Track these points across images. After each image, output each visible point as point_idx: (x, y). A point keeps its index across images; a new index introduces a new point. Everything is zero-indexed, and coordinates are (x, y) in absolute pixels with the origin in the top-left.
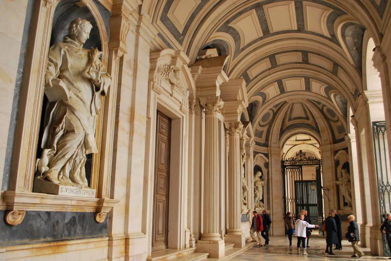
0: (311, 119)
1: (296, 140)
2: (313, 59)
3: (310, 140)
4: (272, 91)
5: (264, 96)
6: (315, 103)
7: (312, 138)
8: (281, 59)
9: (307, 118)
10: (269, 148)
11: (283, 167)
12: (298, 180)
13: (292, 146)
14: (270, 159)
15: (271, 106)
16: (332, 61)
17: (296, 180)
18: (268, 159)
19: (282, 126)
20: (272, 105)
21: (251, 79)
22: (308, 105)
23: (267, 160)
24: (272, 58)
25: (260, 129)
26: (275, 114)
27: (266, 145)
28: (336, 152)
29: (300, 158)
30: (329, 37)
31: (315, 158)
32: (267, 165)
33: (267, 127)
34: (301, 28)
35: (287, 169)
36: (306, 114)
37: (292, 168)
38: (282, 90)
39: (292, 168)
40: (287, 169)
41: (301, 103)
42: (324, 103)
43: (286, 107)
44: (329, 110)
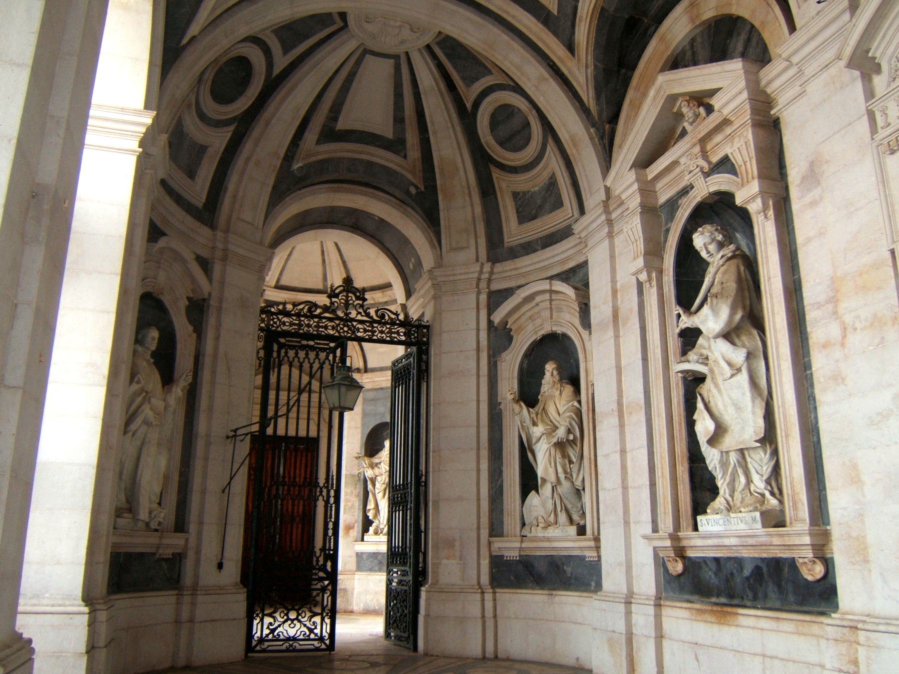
0: (414, 152)
9: (396, 145)
10: (219, 234)
11: (270, 337)
18: (210, 279)
19: (290, 156)
28: (496, 298)
32: (198, 309)
36: (399, 120)
40: (281, 346)
43: (331, 59)
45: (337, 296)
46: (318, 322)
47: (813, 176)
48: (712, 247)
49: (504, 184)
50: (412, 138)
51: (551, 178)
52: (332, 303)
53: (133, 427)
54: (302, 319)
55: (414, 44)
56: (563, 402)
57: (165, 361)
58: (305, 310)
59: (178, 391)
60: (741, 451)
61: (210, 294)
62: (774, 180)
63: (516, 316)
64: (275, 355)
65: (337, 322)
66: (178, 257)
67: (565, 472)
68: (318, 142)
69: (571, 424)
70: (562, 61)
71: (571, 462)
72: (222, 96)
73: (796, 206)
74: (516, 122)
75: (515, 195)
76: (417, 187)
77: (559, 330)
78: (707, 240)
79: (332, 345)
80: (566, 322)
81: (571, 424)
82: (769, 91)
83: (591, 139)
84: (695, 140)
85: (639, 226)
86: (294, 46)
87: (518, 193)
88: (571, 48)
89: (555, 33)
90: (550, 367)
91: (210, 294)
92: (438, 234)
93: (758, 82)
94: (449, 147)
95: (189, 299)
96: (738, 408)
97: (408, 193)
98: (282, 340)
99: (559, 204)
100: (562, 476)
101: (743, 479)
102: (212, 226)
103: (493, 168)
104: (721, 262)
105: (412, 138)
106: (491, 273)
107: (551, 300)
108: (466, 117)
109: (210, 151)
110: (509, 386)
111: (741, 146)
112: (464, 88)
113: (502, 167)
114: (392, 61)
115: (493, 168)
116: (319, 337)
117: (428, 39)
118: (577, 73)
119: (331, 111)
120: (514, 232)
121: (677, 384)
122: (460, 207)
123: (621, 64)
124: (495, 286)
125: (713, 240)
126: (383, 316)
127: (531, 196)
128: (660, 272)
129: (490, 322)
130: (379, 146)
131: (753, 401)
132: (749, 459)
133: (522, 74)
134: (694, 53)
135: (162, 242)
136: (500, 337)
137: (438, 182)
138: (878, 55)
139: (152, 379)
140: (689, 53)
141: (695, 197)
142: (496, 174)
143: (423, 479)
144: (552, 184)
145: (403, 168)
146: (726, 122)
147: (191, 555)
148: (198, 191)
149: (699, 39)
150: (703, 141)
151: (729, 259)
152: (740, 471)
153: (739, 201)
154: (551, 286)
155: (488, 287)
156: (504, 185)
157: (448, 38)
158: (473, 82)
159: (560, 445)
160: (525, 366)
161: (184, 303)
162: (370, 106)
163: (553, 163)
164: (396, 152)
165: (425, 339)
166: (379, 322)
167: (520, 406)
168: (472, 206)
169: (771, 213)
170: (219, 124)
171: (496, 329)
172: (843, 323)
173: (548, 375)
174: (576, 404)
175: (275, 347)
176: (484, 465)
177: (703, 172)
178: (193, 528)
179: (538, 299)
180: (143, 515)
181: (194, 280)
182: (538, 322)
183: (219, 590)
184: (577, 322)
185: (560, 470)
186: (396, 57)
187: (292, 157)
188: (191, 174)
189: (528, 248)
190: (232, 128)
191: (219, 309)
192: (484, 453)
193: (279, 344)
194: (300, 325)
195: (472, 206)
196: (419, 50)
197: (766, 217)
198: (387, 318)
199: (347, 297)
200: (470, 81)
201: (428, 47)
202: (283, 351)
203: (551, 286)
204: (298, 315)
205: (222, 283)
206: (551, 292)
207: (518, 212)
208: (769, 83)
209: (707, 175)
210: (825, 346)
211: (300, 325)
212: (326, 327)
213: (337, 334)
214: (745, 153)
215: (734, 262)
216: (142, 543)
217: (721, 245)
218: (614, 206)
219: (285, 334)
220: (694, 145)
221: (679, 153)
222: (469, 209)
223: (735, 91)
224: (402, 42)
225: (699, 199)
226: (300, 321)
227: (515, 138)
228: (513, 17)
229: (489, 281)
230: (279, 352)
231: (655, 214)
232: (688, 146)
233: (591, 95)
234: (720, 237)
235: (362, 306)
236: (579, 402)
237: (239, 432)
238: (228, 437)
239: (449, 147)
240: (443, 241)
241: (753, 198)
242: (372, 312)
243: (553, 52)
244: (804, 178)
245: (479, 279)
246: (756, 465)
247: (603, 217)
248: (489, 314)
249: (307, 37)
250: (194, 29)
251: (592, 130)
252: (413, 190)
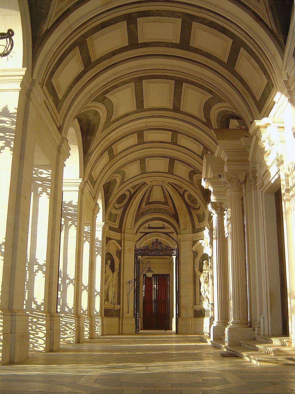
1: (149, 228)
2: (183, 141)
3: (164, 228)
4: (133, 170)
5: (124, 175)
6: (174, 186)
7: (166, 225)
8: (150, 136)
9: (166, 203)
13: (142, 234)
15: (128, 187)
16: (203, 144)
18: (121, 246)
20: (131, 185)
21: (115, 154)
22: (169, 189)
24: (140, 134)
25: (114, 212)
26: (132, 196)
27: (120, 230)
30: (204, 120)
32: (119, 253)
34: (176, 109)
36: (165, 197)
38: (143, 171)
41: (162, 187)
42: (186, 188)
43: (145, 189)
44: (190, 196)
49: (193, 212)
52: (153, 246)
53: (106, 283)
57: (112, 267)
59: (116, 273)
61: (121, 249)
76: (173, 213)
91: (121, 249)
94: (179, 203)
97: (171, 214)
108: (182, 196)
122: (184, 218)
139: (109, 271)
145: (169, 209)
147: (121, 309)
162: (157, 195)
166: (165, 250)
178: (121, 303)
180: (110, 301)
181: (117, 247)
183: (128, 318)
188: (115, 222)
191: (124, 252)
216: (111, 307)
235: (161, 246)
239: (179, 203)
242: (164, 248)
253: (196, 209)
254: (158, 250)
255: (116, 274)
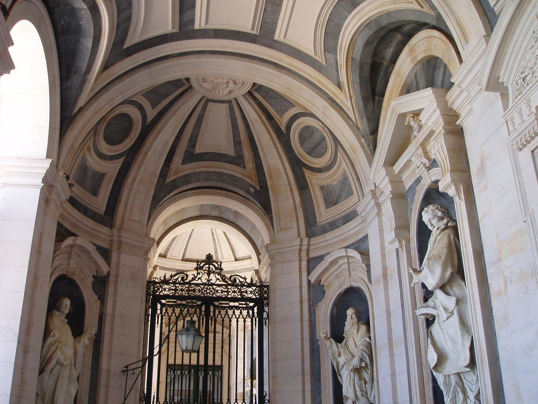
0: (250, 165)
12: (178, 362)
14: (113, 266)
17: (171, 362)
18: (109, 263)
23: (105, 268)
28: (313, 262)
29: (206, 276)
31: (249, 281)
32: (101, 284)
33: (118, 163)
35: (163, 305)
36: (237, 143)
37: (178, 306)
39: (178, 306)
44: (307, 133)
45: (201, 268)
46: (188, 287)
47: (482, 168)
48: (434, 222)
49: (315, 181)
50: (247, 154)
51: (344, 174)
52: (198, 273)
54: (177, 285)
55: (240, 92)
56: (359, 338)
58: (180, 279)
59: (86, 340)
60: (458, 374)
61: (109, 273)
62: (462, 171)
63: (327, 275)
64: (159, 312)
65: (202, 286)
66: (83, 249)
67: (362, 391)
68: (183, 163)
69: (362, 355)
70: (335, 95)
71: (366, 383)
72: (111, 141)
73: (476, 190)
74: (316, 138)
75: (322, 188)
76: (255, 188)
77: (355, 284)
78: (431, 217)
79: (199, 303)
80: (358, 279)
81: (362, 355)
82: (455, 109)
83: (362, 146)
84: (417, 145)
85: (391, 208)
86: (159, 102)
87: (324, 187)
88: (339, 86)
89: (328, 77)
90: (350, 312)
91: (109, 273)
92: (271, 219)
93: (446, 102)
95: (93, 276)
96: (454, 342)
98: (163, 301)
99: (352, 193)
100: (359, 393)
101: (461, 396)
102: (111, 227)
103: (304, 170)
104: (437, 233)
105: (247, 154)
106: (309, 245)
107: (349, 263)
108: (282, 136)
109: (108, 176)
110: (324, 328)
111: (439, 149)
112: (278, 118)
113: (312, 169)
114: (227, 105)
115: (304, 170)
116: (189, 297)
117: (247, 88)
118: (346, 102)
119: (190, 141)
120: (324, 214)
121: (423, 324)
123: (374, 94)
124: (312, 255)
125: (435, 216)
126: (235, 280)
127: (333, 188)
128: (408, 241)
129: (309, 281)
130: (225, 162)
131: (463, 337)
132: (464, 381)
133: (313, 105)
134: (417, 83)
135: (69, 241)
136: (316, 290)
137: (268, 183)
138: (505, 81)
140: (414, 83)
141: (424, 185)
142: (308, 174)
143: (267, 398)
144: (345, 179)
146: (432, 133)
148: (100, 203)
149: (419, 73)
150: (423, 145)
151: (443, 230)
152: (459, 389)
153: (441, 189)
154: (347, 253)
155: (308, 254)
156: (314, 182)
157: (261, 86)
158: (284, 113)
159: (357, 370)
160: (335, 312)
161: (90, 281)
163: (343, 165)
164: (238, 165)
165: (265, 295)
166: (232, 285)
167: (331, 342)
168: (293, 197)
169: (463, 196)
170: (112, 158)
171: (313, 285)
172: (504, 277)
173: (349, 318)
174: (367, 339)
175: (159, 306)
176: (308, 387)
177: (426, 167)
179: (340, 262)
181: (96, 264)
182: (342, 279)
184: (366, 278)
185: (358, 389)
186: (229, 102)
187: (166, 175)
188: (95, 192)
189: (333, 225)
190: (122, 160)
191: (116, 283)
192: (308, 378)
193: (161, 303)
194: (176, 290)
195: (293, 197)
196: (243, 96)
197: (460, 198)
198: (238, 281)
199: (209, 268)
200: (282, 112)
201: (249, 92)
202: (164, 309)
203: (347, 253)
204: (174, 283)
205: (118, 264)
206: (348, 257)
207: (325, 200)
208: (453, 102)
209: (429, 169)
210: (499, 294)
211: (176, 290)
212: (194, 291)
213: (202, 295)
214: (442, 153)
215: (447, 231)
217: (441, 219)
218: (379, 193)
219: (165, 297)
220: (418, 148)
221: (410, 154)
222: (291, 200)
223: (431, 110)
224: (230, 92)
225: (426, 187)
226: (176, 287)
227: (316, 150)
228: (298, 69)
229: (308, 250)
230: (161, 310)
231: (401, 197)
232: (414, 149)
233: (357, 116)
234: (440, 214)
235: (219, 274)
236: (370, 338)
237: (130, 368)
238: (123, 371)
240: (275, 224)
241: (449, 186)
243: (328, 89)
244: (479, 169)
245: (300, 250)
246: (470, 385)
247: (373, 202)
248: (309, 274)
249: (167, 96)
250: (81, 103)
251: (363, 140)
252: (252, 190)
253: (319, 170)
254: (212, 284)
255: (87, 342)
